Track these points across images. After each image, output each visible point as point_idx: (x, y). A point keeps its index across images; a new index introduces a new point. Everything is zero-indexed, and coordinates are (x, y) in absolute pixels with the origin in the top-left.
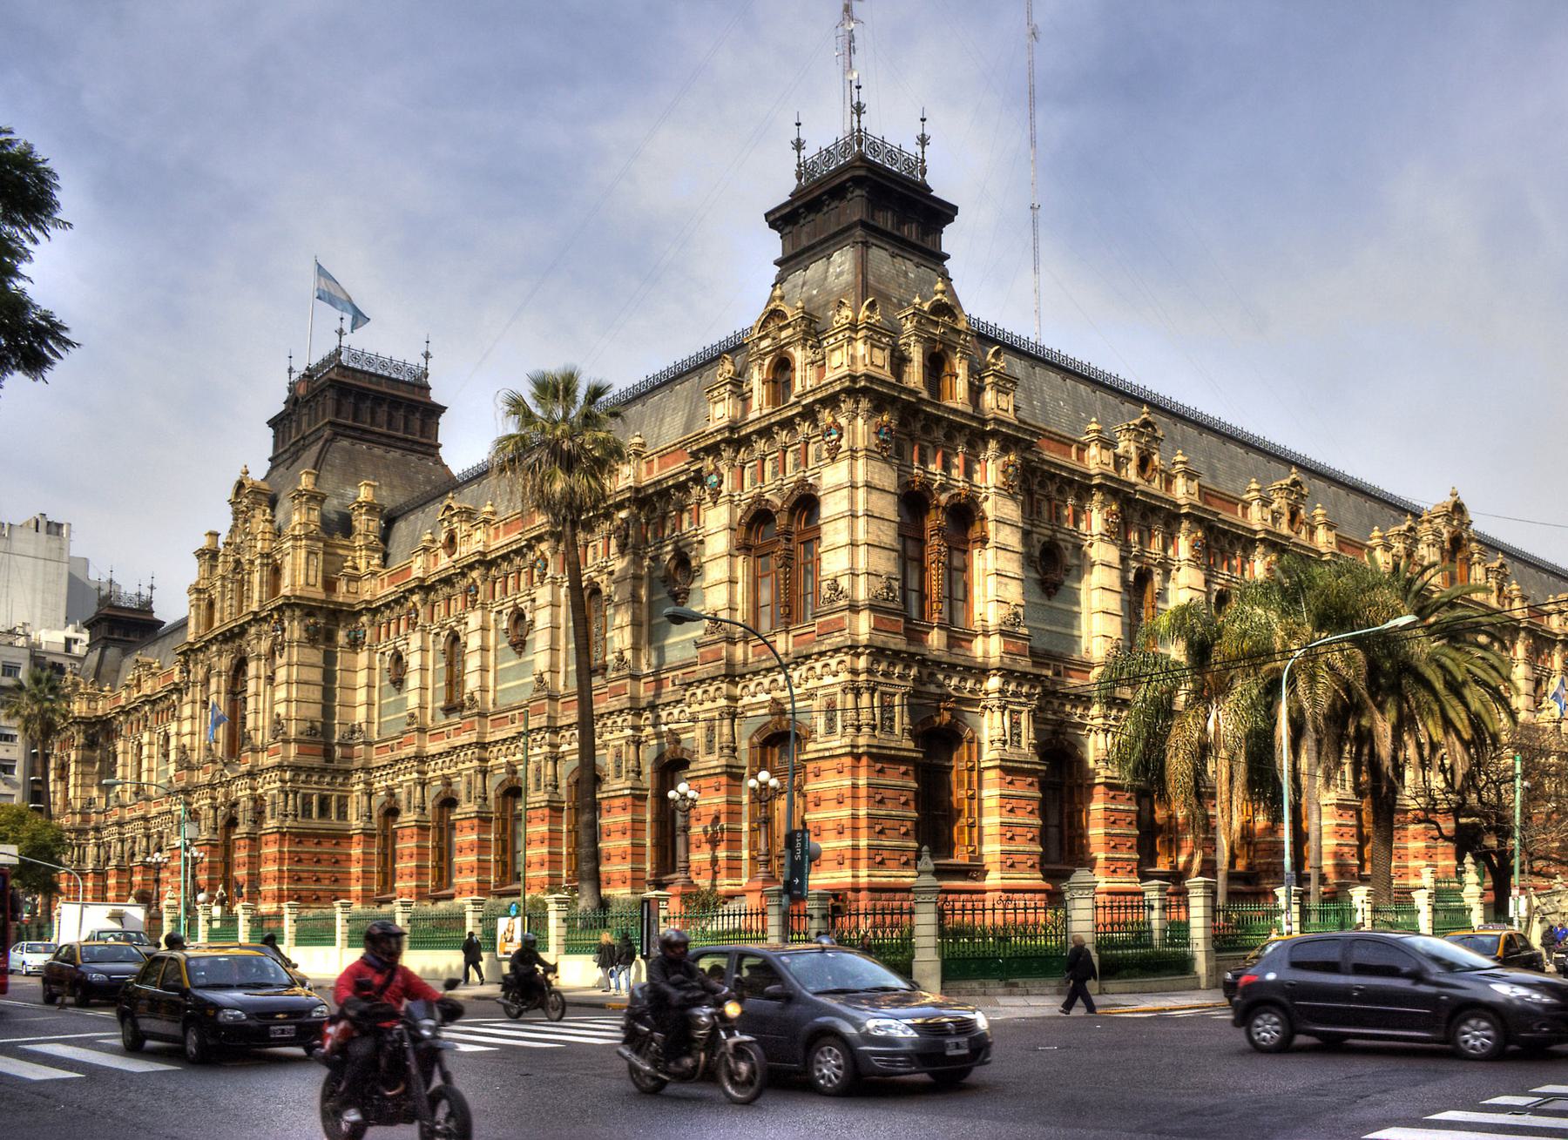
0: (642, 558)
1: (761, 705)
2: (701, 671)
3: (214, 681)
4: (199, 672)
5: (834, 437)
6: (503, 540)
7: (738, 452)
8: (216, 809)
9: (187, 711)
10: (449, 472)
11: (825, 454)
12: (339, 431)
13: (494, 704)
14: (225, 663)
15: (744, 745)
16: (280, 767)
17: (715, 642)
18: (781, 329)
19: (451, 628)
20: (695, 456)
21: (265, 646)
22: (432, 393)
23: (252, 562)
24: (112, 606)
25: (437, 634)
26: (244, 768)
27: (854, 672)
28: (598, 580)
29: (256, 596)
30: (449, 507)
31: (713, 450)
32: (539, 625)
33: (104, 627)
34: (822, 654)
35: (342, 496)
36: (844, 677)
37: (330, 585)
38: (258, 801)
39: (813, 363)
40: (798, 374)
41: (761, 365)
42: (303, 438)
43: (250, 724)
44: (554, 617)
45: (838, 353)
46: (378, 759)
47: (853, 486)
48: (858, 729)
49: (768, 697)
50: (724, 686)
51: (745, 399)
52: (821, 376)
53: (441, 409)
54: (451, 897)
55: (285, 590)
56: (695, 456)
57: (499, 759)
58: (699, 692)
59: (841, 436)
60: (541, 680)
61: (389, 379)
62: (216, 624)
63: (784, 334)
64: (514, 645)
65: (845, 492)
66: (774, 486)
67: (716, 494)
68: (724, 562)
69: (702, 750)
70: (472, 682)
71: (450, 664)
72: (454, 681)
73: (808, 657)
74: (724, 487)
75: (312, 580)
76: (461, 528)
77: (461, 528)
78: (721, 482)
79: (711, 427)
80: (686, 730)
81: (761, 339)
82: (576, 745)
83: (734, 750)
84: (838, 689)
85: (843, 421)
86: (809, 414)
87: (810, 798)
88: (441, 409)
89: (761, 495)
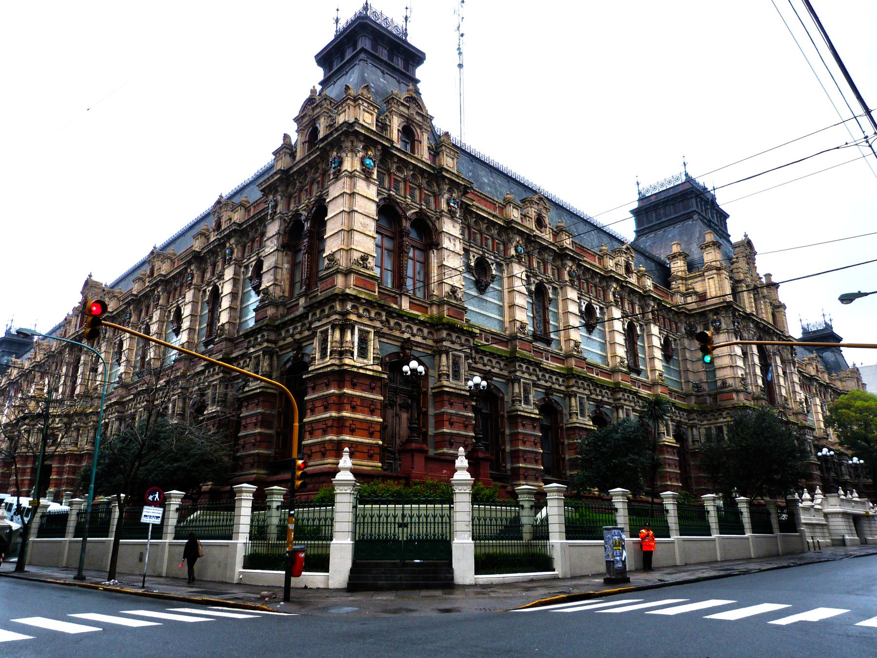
0: (240, 267)
7: (287, 187)
18: (313, 109)
50: (265, 333)
63: (315, 112)
66: (304, 206)
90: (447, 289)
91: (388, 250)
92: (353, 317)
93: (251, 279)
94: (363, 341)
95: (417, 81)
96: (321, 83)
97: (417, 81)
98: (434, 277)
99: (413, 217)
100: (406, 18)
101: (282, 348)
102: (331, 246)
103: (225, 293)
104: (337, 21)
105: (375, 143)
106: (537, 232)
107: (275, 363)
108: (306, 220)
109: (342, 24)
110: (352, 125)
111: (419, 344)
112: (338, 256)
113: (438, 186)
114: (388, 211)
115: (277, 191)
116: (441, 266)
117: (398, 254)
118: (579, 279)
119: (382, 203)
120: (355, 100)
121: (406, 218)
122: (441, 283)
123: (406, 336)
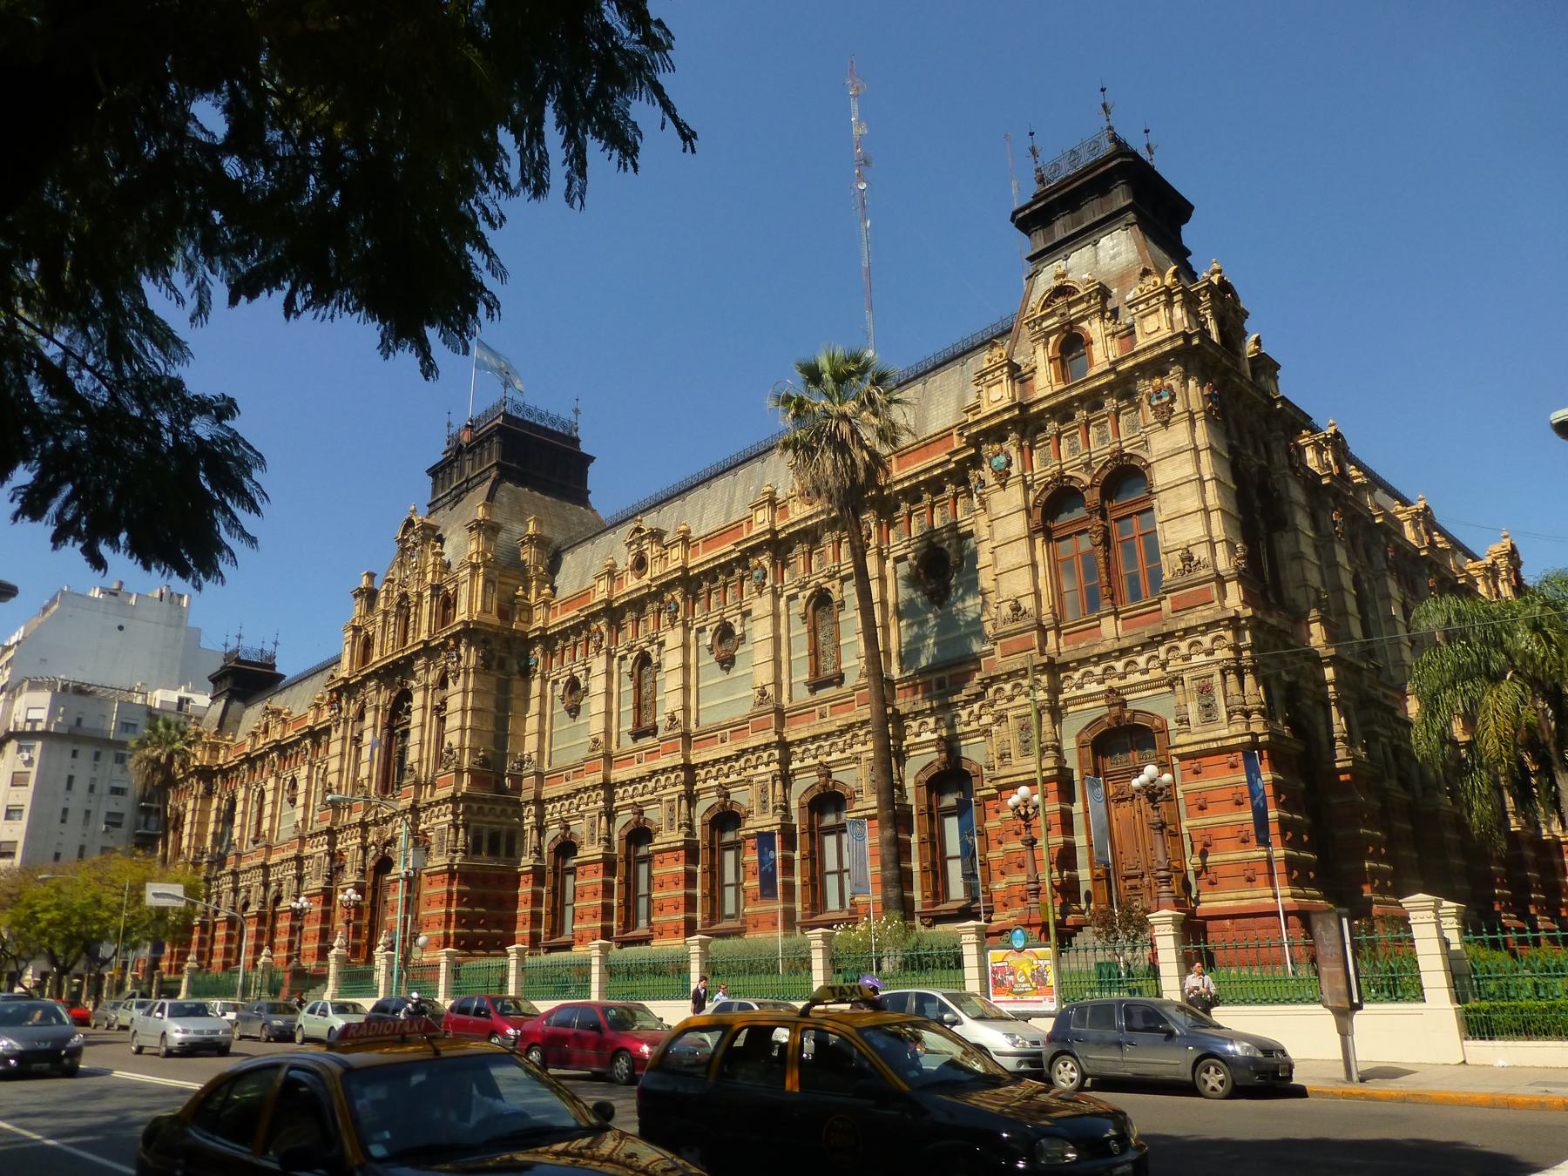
1: (1091, 697)
5: (1167, 399)
10: (598, 517)
12: (505, 474)
13: (791, 699)
14: (378, 698)
15: (1069, 744)
16: (453, 799)
18: (1070, 305)
19: (642, 651)
21: (433, 676)
22: (582, 445)
23: (420, 595)
24: (238, 660)
25: (623, 658)
27: (1237, 650)
28: (828, 585)
29: (425, 626)
30: (639, 530)
31: (997, 434)
33: (227, 684)
34: (1188, 631)
35: (510, 531)
36: (1223, 654)
37: (504, 614)
39: (1113, 335)
41: (1046, 344)
42: (467, 481)
46: (548, 792)
47: (1196, 450)
48: (1247, 714)
53: (592, 459)
57: (707, 782)
61: (546, 429)
62: (410, 642)
64: (569, 711)
68: (1023, 546)
71: (638, 687)
72: (643, 704)
75: (488, 608)
76: (651, 551)
77: (651, 551)
78: (1009, 463)
81: (1044, 318)
82: (870, 745)
84: (1216, 669)
85: (1175, 384)
88: (592, 459)
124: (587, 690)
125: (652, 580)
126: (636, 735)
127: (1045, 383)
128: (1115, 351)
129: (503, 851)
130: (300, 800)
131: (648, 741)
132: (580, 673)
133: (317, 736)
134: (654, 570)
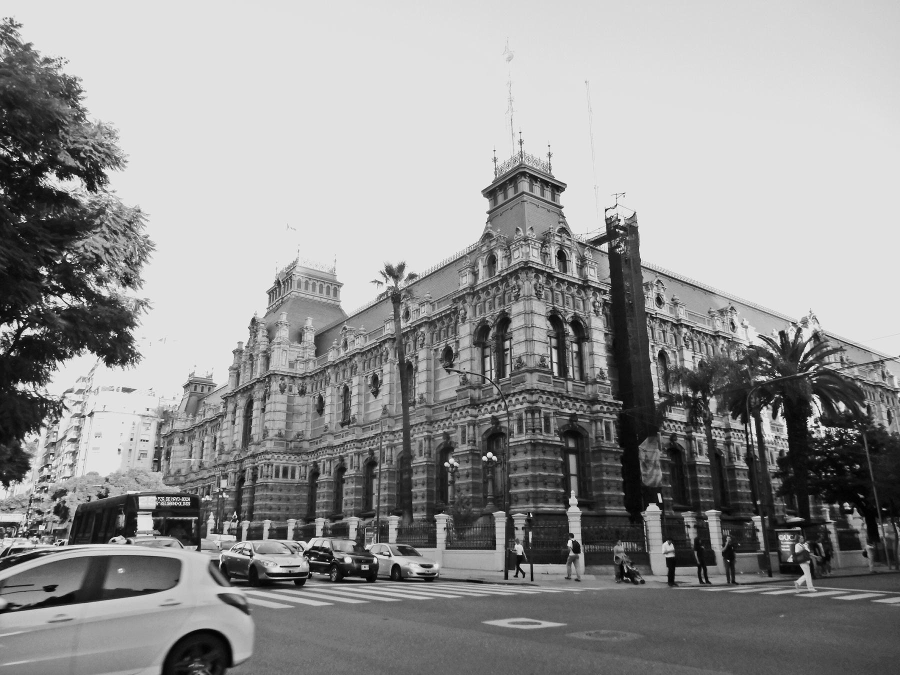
1: (487, 420)
2: (459, 404)
3: (238, 412)
4: (231, 407)
6: (369, 343)
8: (235, 473)
9: (225, 426)
11: (513, 298)
14: (242, 402)
17: (464, 389)
18: (490, 242)
20: (454, 301)
26: (249, 453)
31: (462, 298)
32: (384, 382)
34: (514, 394)
38: (255, 469)
40: (499, 262)
43: (253, 432)
44: (391, 379)
45: (517, 252)
48: (534, 431)
49: (490, 416)
50: (469, 410)
51: (475, 274)
52: (509, 263)
54: (341, 518)
55: (271, 368)
56: (454, 301)
58: (458, 413)
59: (519, 289)
60: (385, 409)
65: (522, 316)
66: (491, 315)
67: (464, 319)
68: (468, 351)
69: (460, 442)
70: (354, 411)
71: (345, 402)
72: (346, 410)
73: (508, 395)
74: (468, 316)
78: (466, 313)
79: (461, 288)
80: (452, 432)
82: (401, 441)
83: (475, 442)
85: (520, 283)
86: (504, 279)
87: (512, 466)
89: (484, 318)
90: (597, 372)
91: (555, 348)
92: (540, 405)
93: (441, 360)
94: (547, 419)
95: (561, 207)
96: (489, 213)
97: (561, 207)
98: (587, 363)
99: (571, 320)
100: (550, 155)
101: (482, 421)
102: (519, 350)
103: (420, 369)
104: (495, 160)
105: (542, 272)
106: (658, 310)
107: (477, 431)
108: (493, 326)
109: (500, 163)
110: (526, 263)
111: (581, 416)
112: (524, 359)
113: (585, 292)
114: (554, 318)
115: (465, 302)
116: (592, 354)
117: (561, 349)
118: (692, 340)
119: (549, 314)
120: (525, 241)
121: (566, 322)
122: (593, 367)
123: (573, 411)
124: (417, 368)
125: (412, 323)
126: (342, 425)
127: (483, 277)
128: (505, 266)
129: (289, 476)
130: (217, 448)
131: (346, 428)
132: (378, 373)
133: (216, 422)
134: (351, 348)
